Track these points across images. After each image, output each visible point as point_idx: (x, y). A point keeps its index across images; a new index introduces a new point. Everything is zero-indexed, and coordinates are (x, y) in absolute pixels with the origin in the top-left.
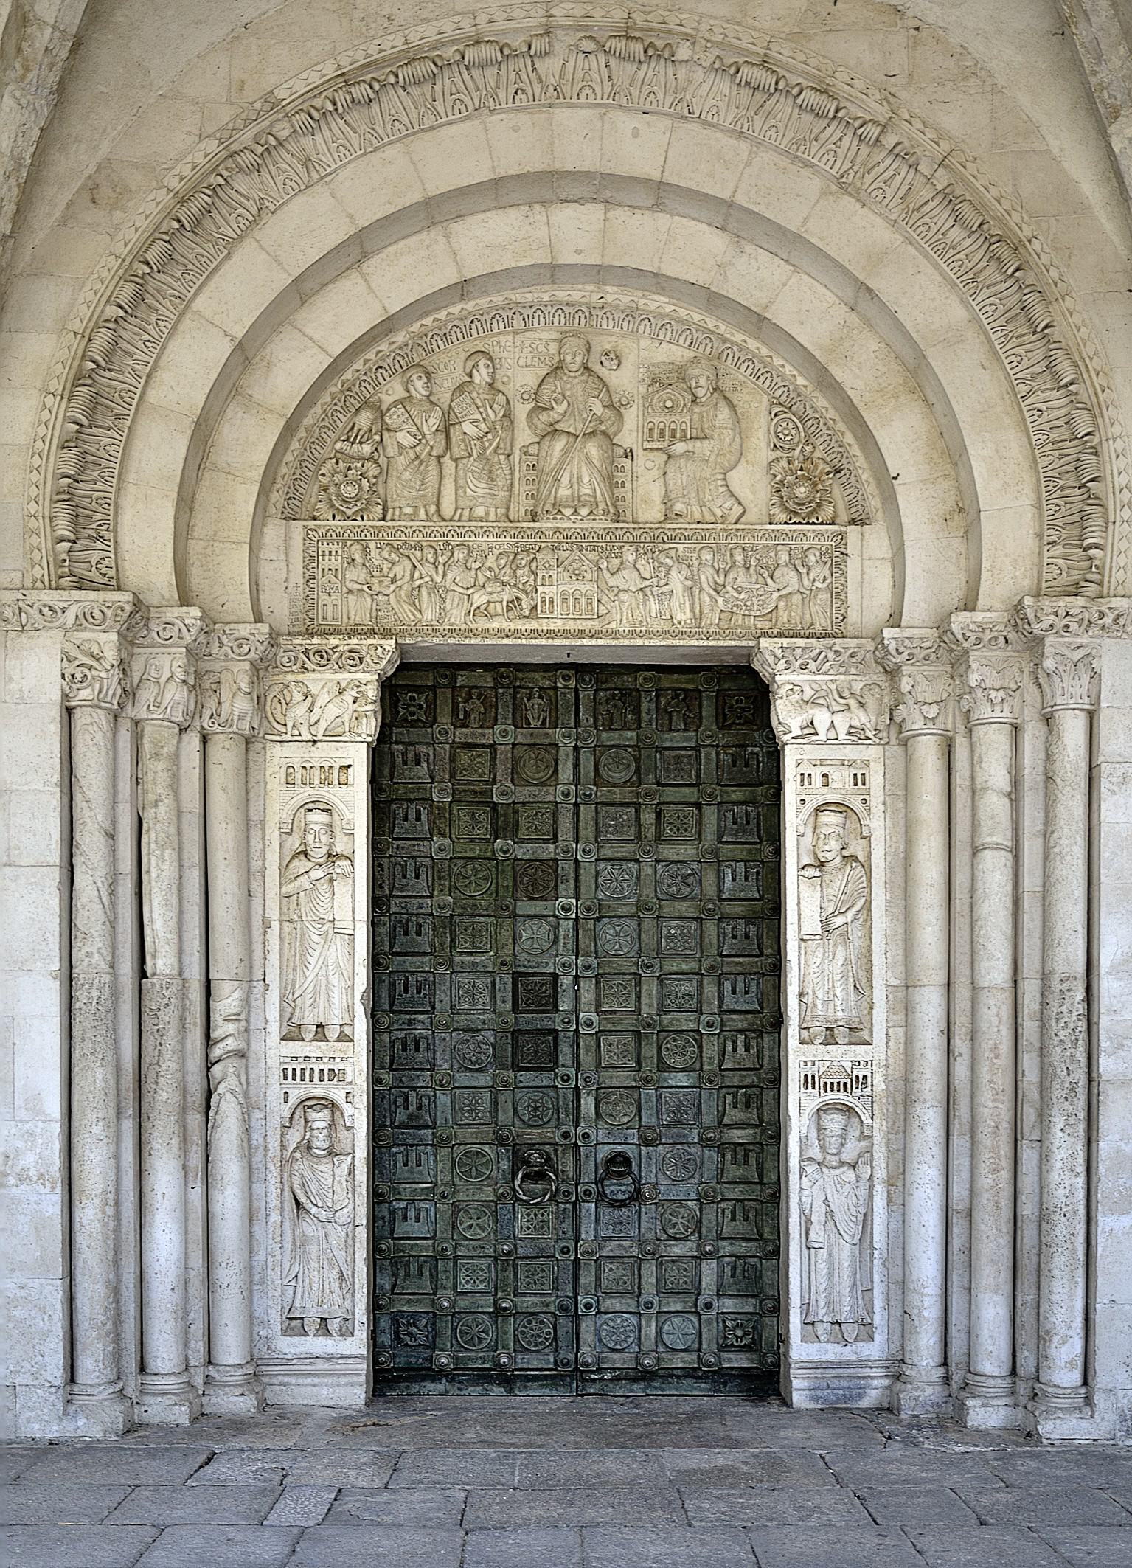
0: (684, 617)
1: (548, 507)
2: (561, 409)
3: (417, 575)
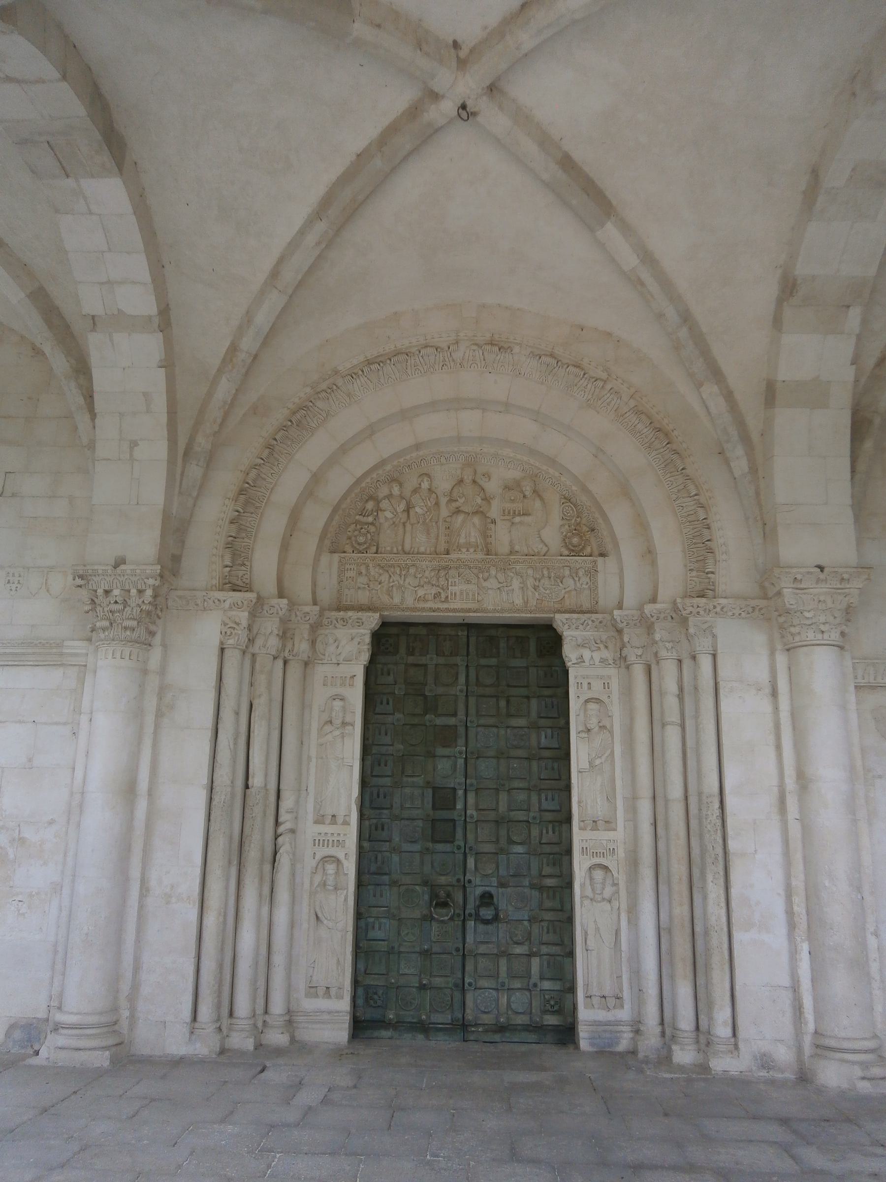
0: (519, 601)
1: (455, 547)
2: (462, 501)
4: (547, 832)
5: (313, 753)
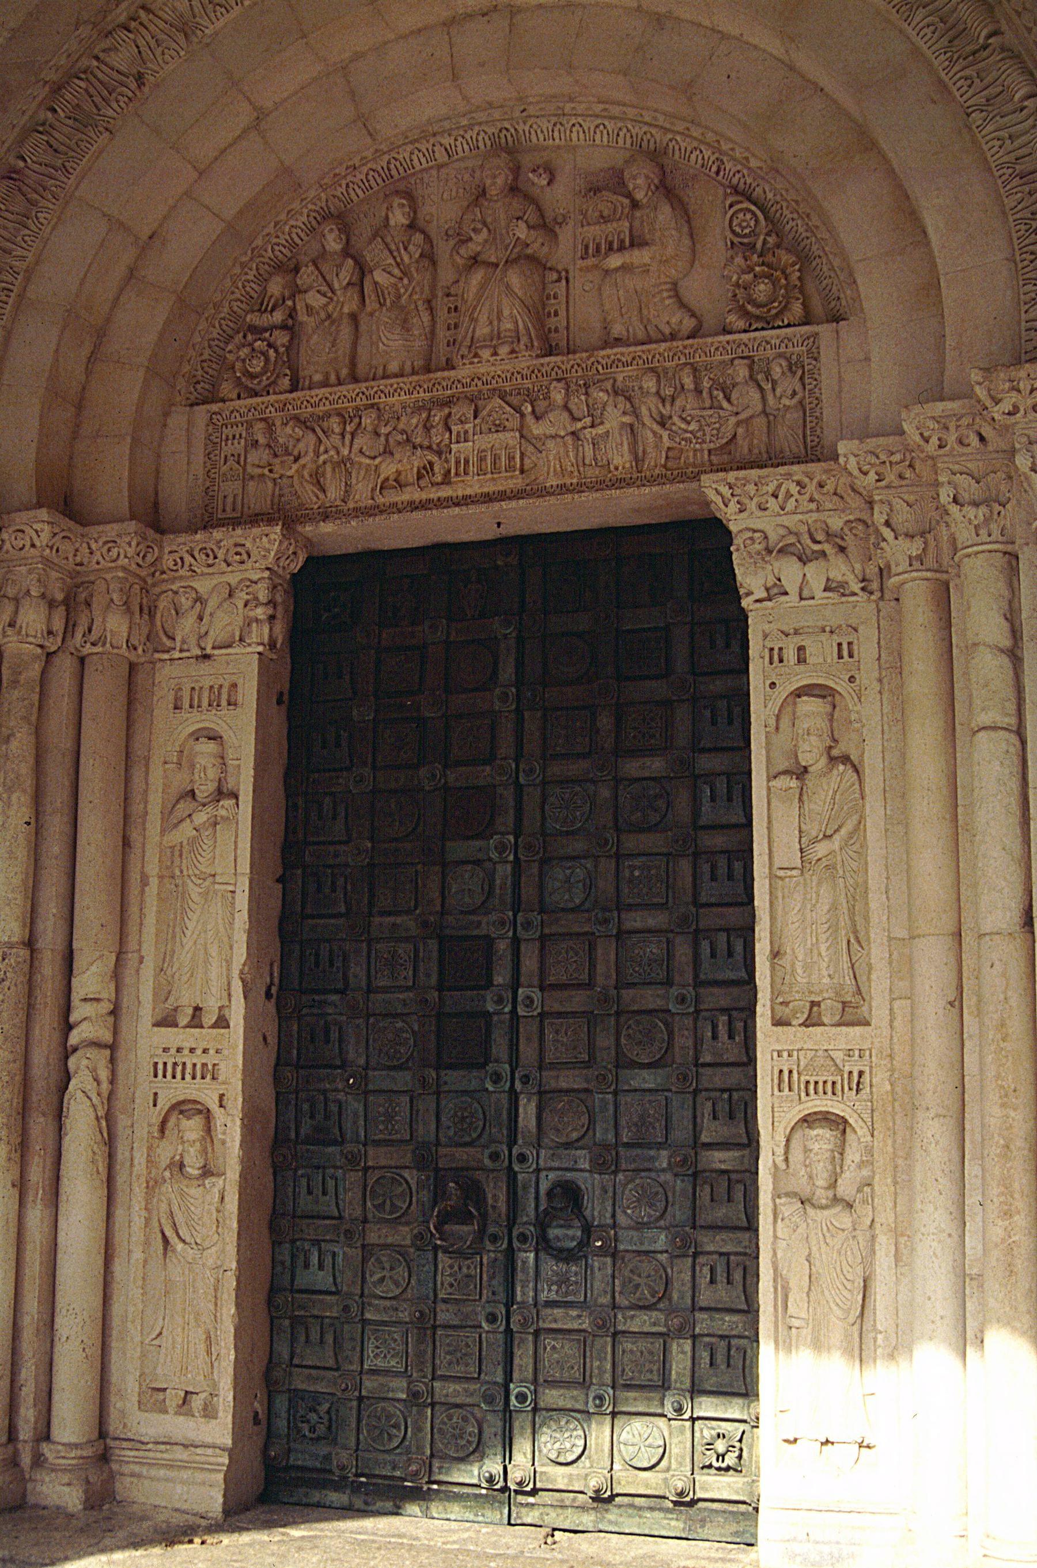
3: (322, 449)
4: (715, 1037)
5: (153, 869)
